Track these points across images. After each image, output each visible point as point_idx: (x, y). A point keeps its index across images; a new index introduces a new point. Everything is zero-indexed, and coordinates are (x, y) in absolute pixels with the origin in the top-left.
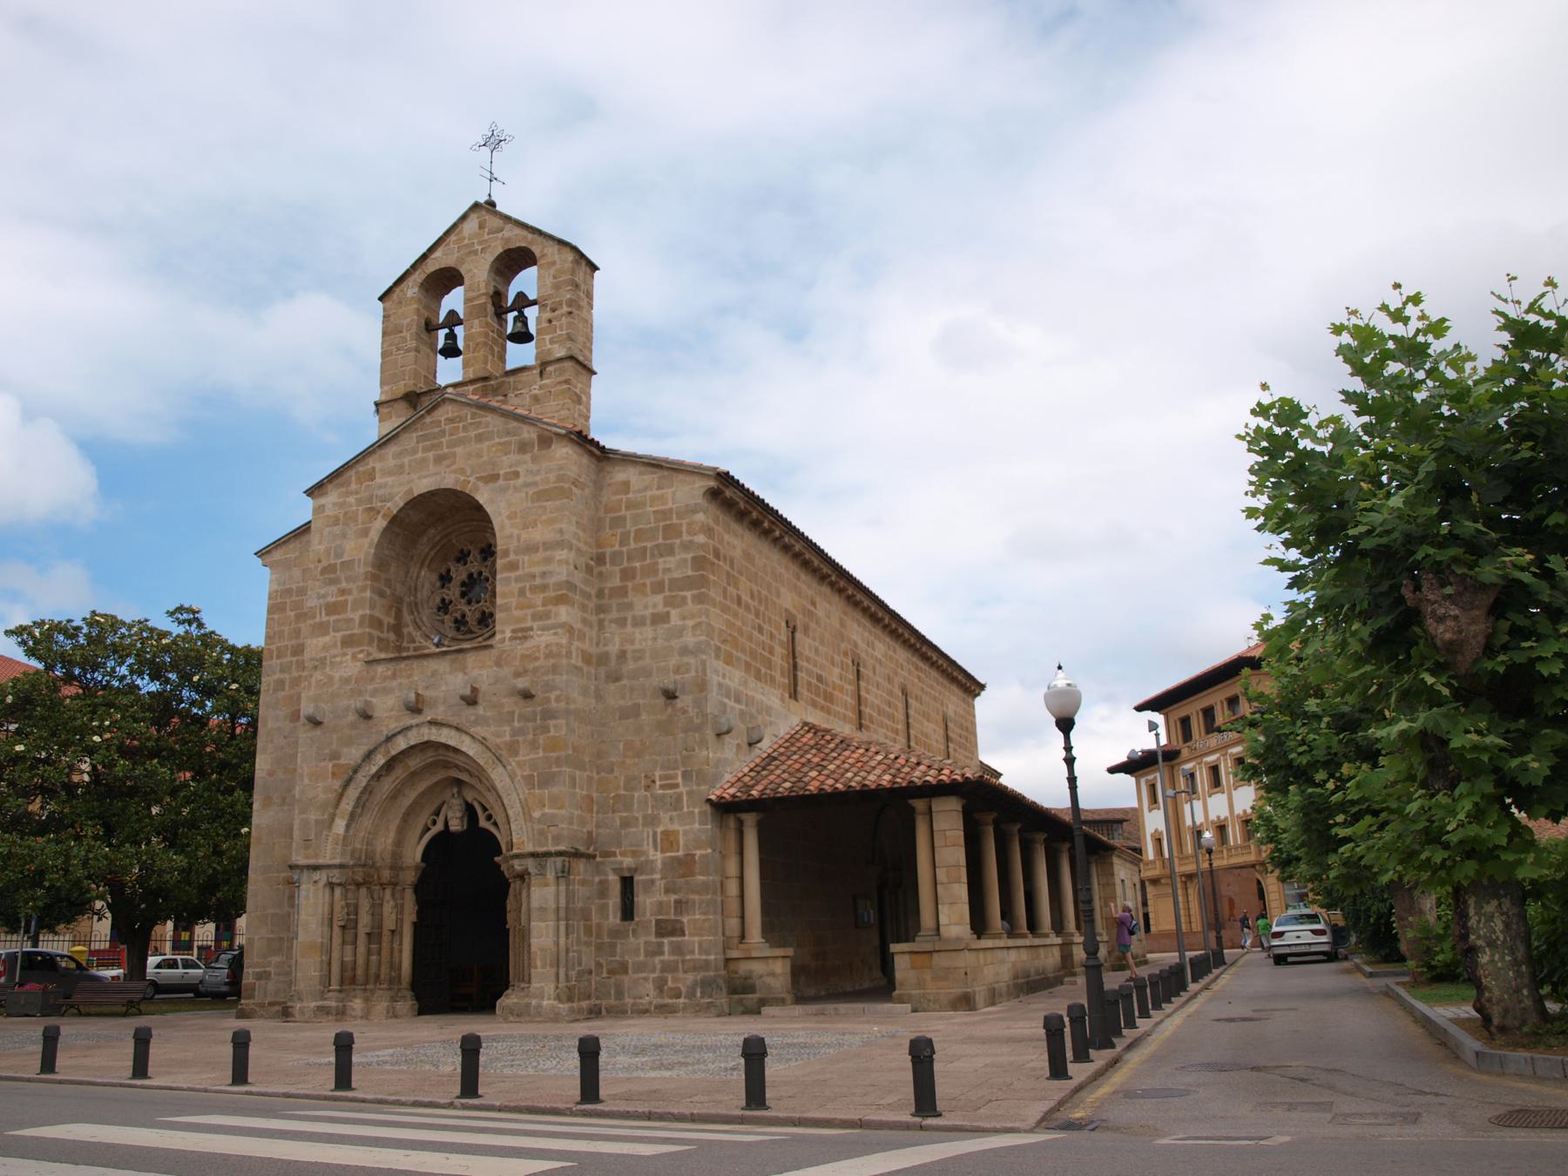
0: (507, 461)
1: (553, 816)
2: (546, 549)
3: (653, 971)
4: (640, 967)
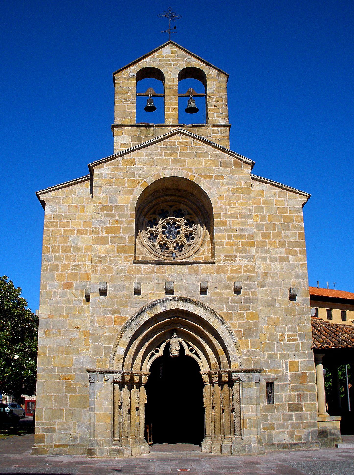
0: (217, 170)
1: (254, 352)
2: (242, 218)
3: (288, 428)
4: (281, 426)
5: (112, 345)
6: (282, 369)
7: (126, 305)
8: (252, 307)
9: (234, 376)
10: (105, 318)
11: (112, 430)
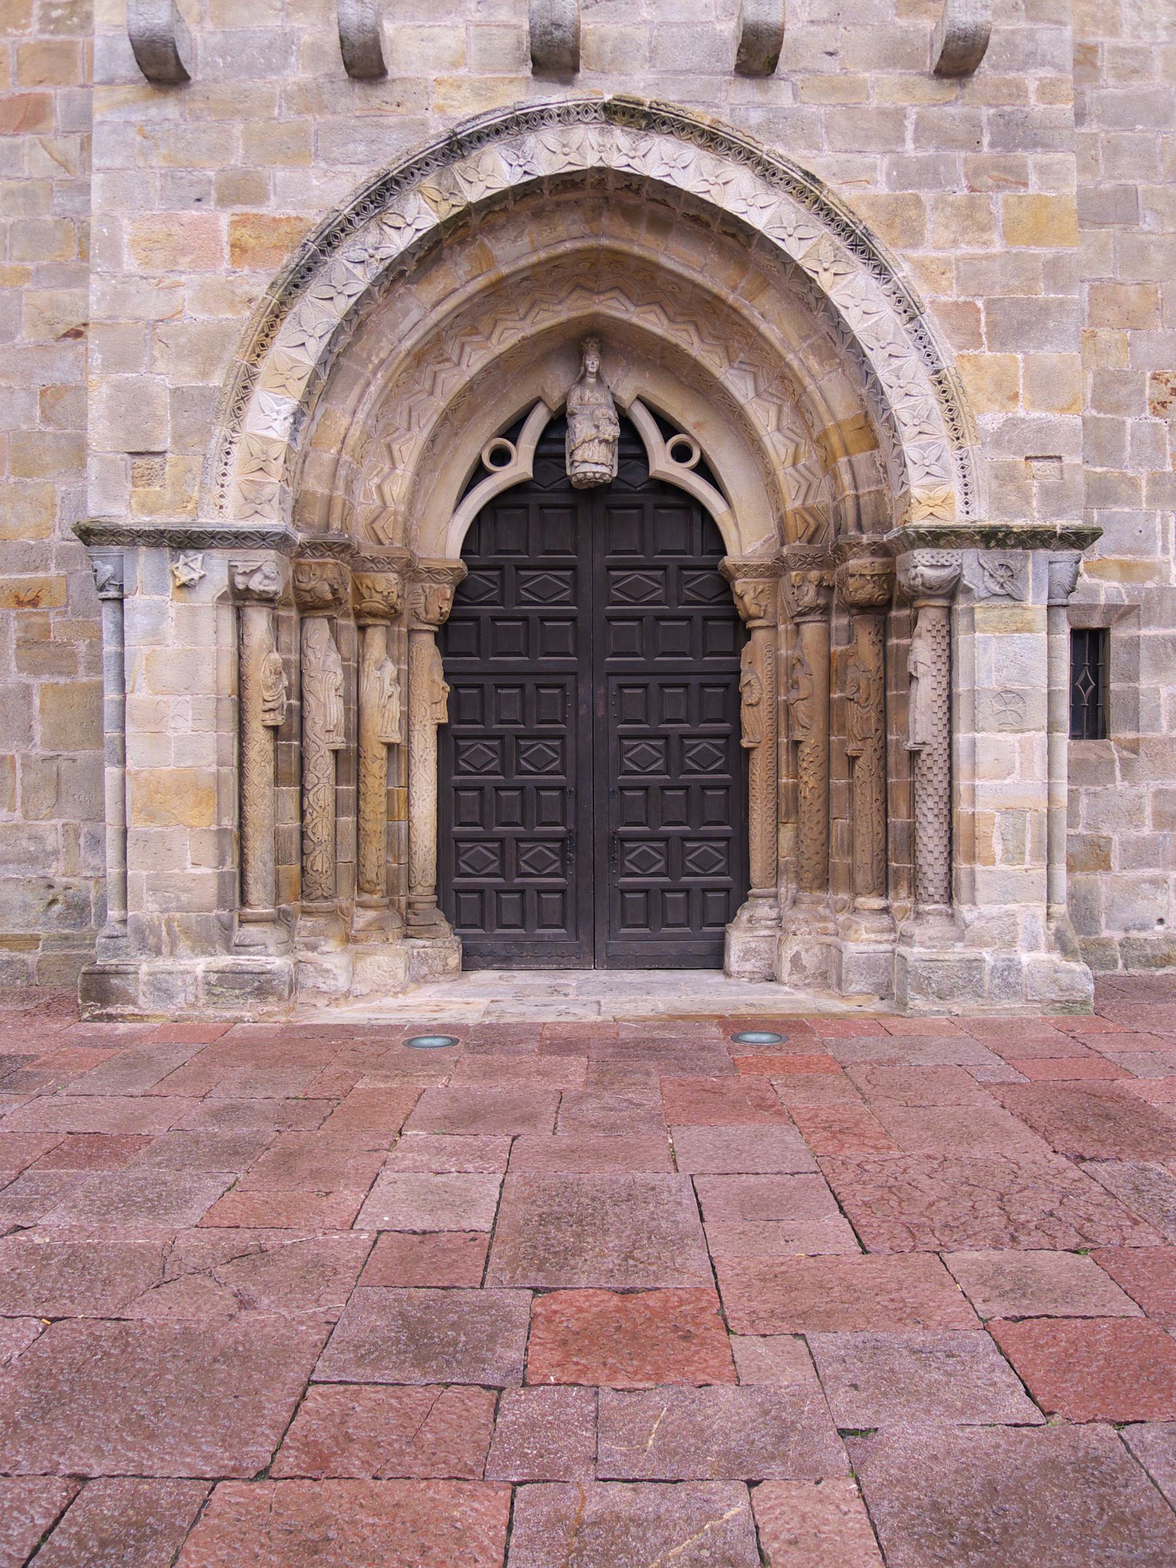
1: (1043, 429)
5: (217, 380)
6: (1159, 556)
7: (297, 149)
8: (1043, 170)
10: (176, 229)
11: (231, 866)
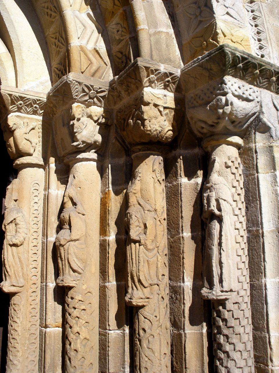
9: (238, 94)
